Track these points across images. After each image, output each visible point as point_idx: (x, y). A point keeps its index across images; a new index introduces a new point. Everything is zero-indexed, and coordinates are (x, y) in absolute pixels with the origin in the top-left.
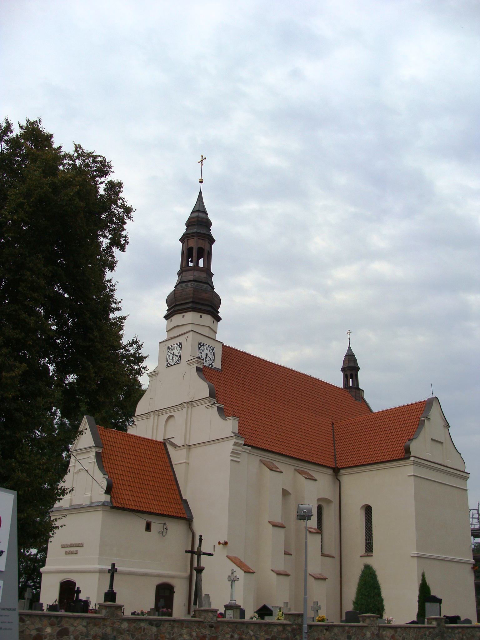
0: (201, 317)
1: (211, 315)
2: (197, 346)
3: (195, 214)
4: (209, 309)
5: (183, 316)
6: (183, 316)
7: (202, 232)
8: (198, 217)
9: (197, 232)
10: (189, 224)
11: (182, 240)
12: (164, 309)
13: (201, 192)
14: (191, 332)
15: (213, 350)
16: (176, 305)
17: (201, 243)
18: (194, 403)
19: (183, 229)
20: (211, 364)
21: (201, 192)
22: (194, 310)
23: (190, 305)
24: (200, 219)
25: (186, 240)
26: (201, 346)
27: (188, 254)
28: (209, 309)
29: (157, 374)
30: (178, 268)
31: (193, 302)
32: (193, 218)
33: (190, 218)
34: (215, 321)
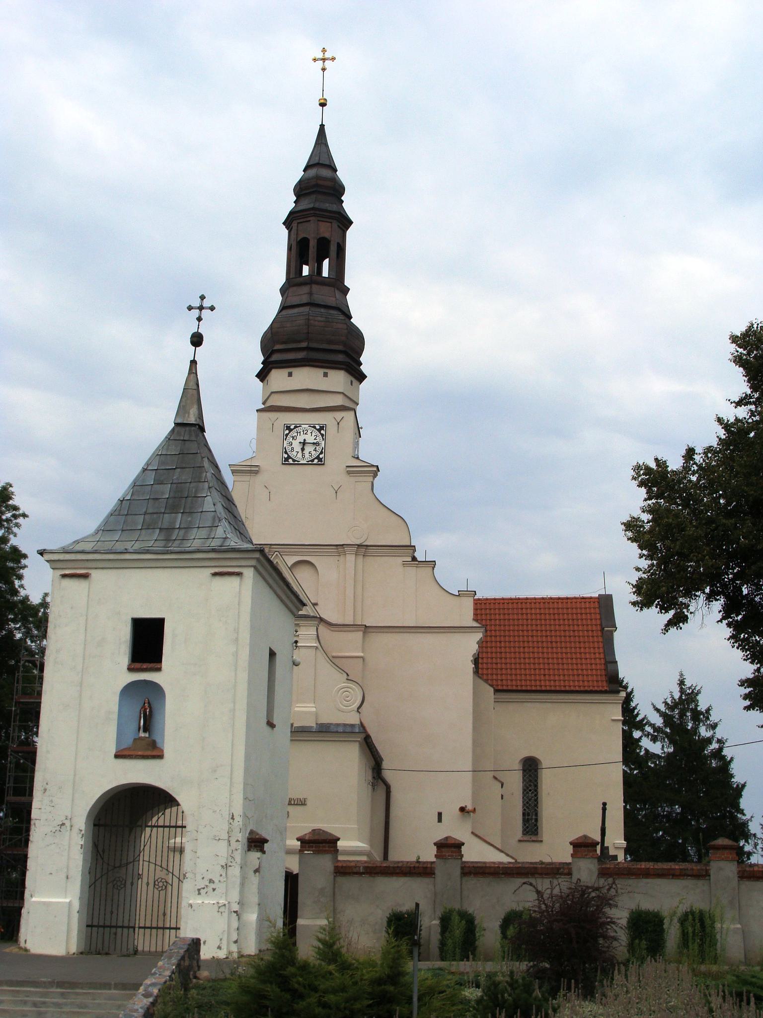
0: (326, 375)
3: (312, 172)
4: (341, 357)
8: (317, 177)
9: (313, 209)
10: (302, 190)
11: (288, 223)
12: (257, 360)
13: (322, 127)
16: (282, 349)
17: (326, 230)
19: (288, 202)
21: (322, 127)
25: (294, 225)
27: (299, 252)
28: (341, 357)
30: (282, 279)
32: (309, 179)
33: (300, 182)
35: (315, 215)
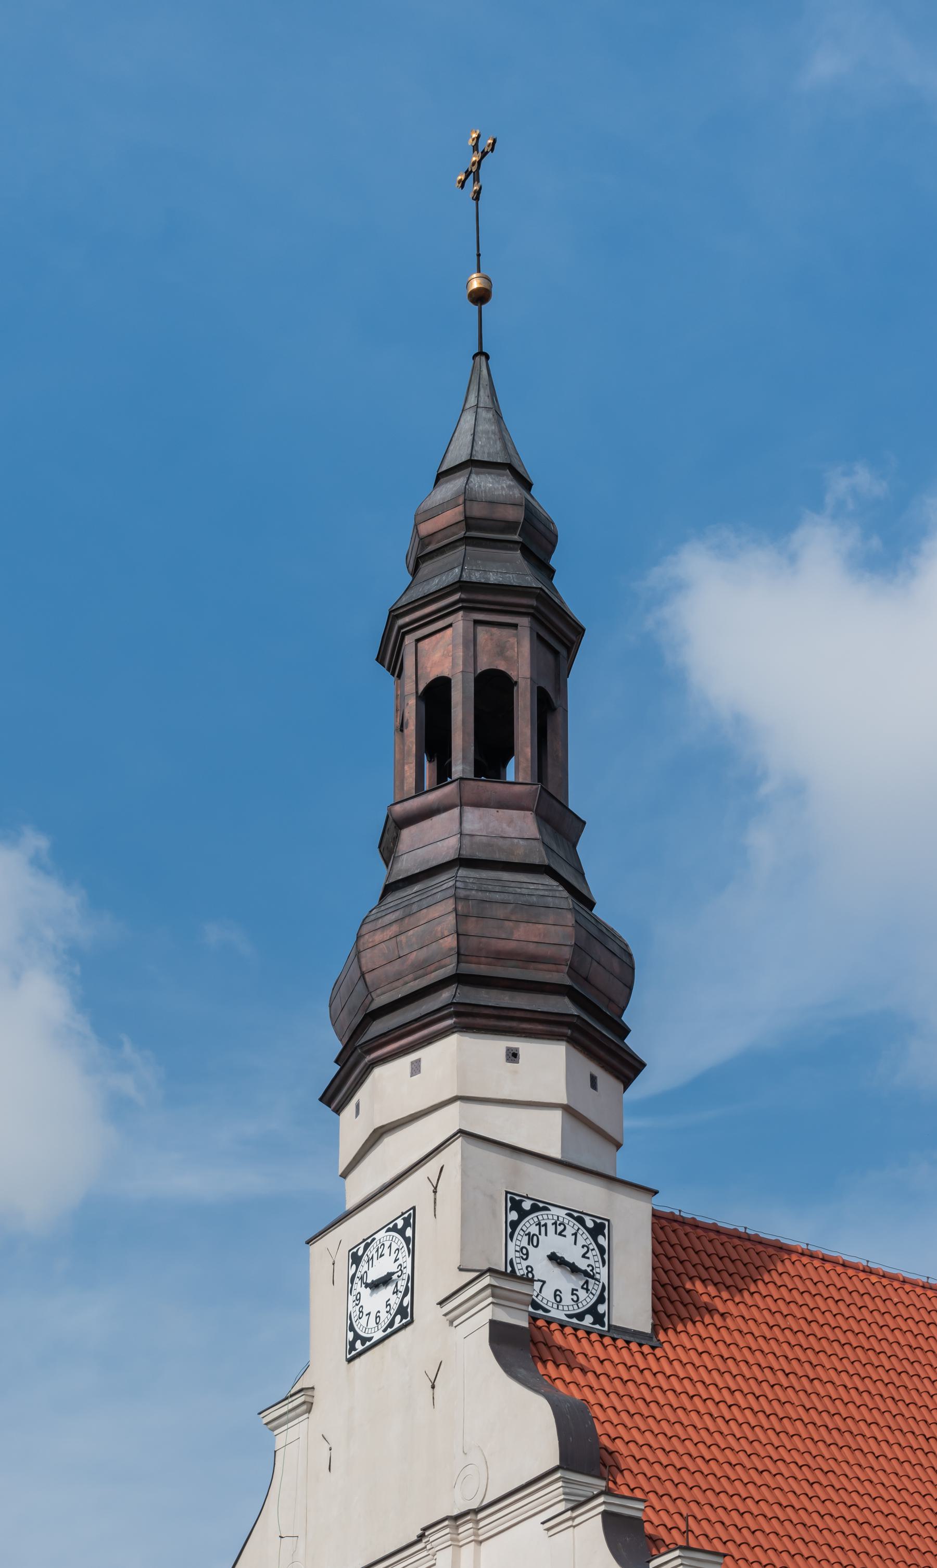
0: (513, 1056)
1: (572, 1041)
2: (502, 1215)
5: (416, 1068)
6: (416, 1068)
7: (493, 578)
9: (461, 585)
14: (458, 1143)
15: (597, 1231)
18: (489, 1522)
20: (592, 1310)
22: (473, 1020)
23: (445, 996)
24: (477, 511)
26: (523, 1214)
29: (309, 1406)
31: (458, 979)
34: (606, 1080)
35: (468, 607)
